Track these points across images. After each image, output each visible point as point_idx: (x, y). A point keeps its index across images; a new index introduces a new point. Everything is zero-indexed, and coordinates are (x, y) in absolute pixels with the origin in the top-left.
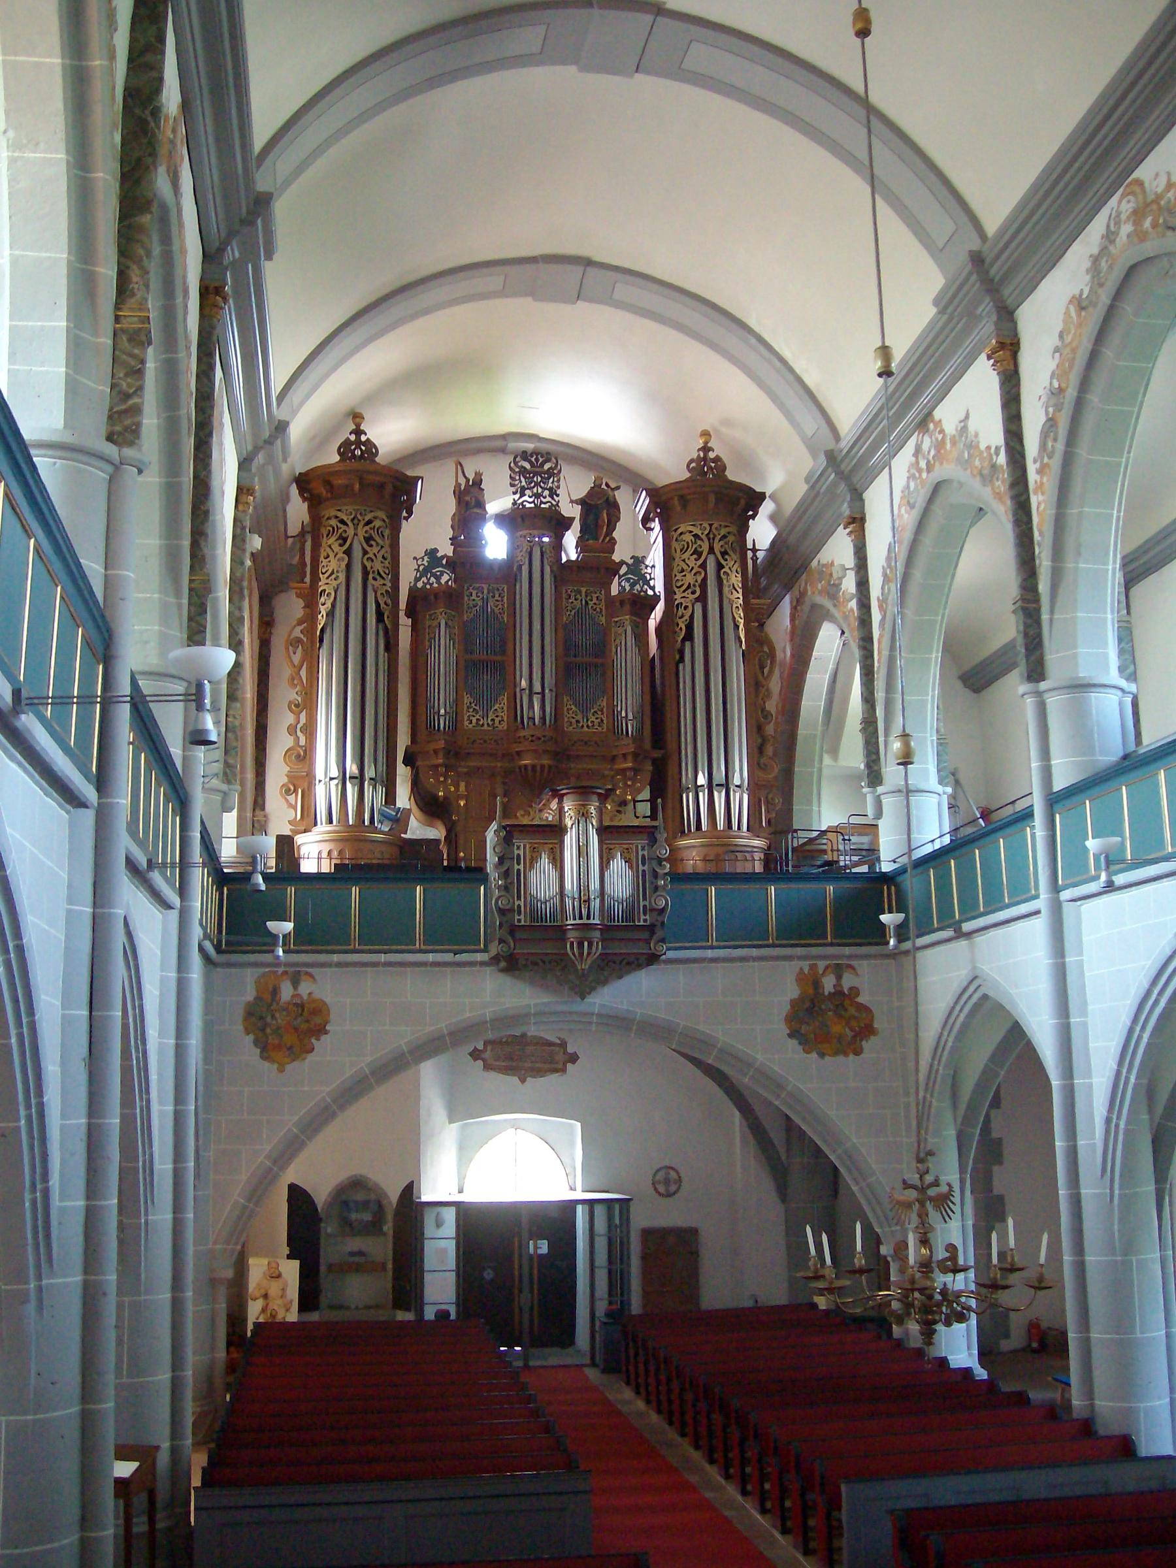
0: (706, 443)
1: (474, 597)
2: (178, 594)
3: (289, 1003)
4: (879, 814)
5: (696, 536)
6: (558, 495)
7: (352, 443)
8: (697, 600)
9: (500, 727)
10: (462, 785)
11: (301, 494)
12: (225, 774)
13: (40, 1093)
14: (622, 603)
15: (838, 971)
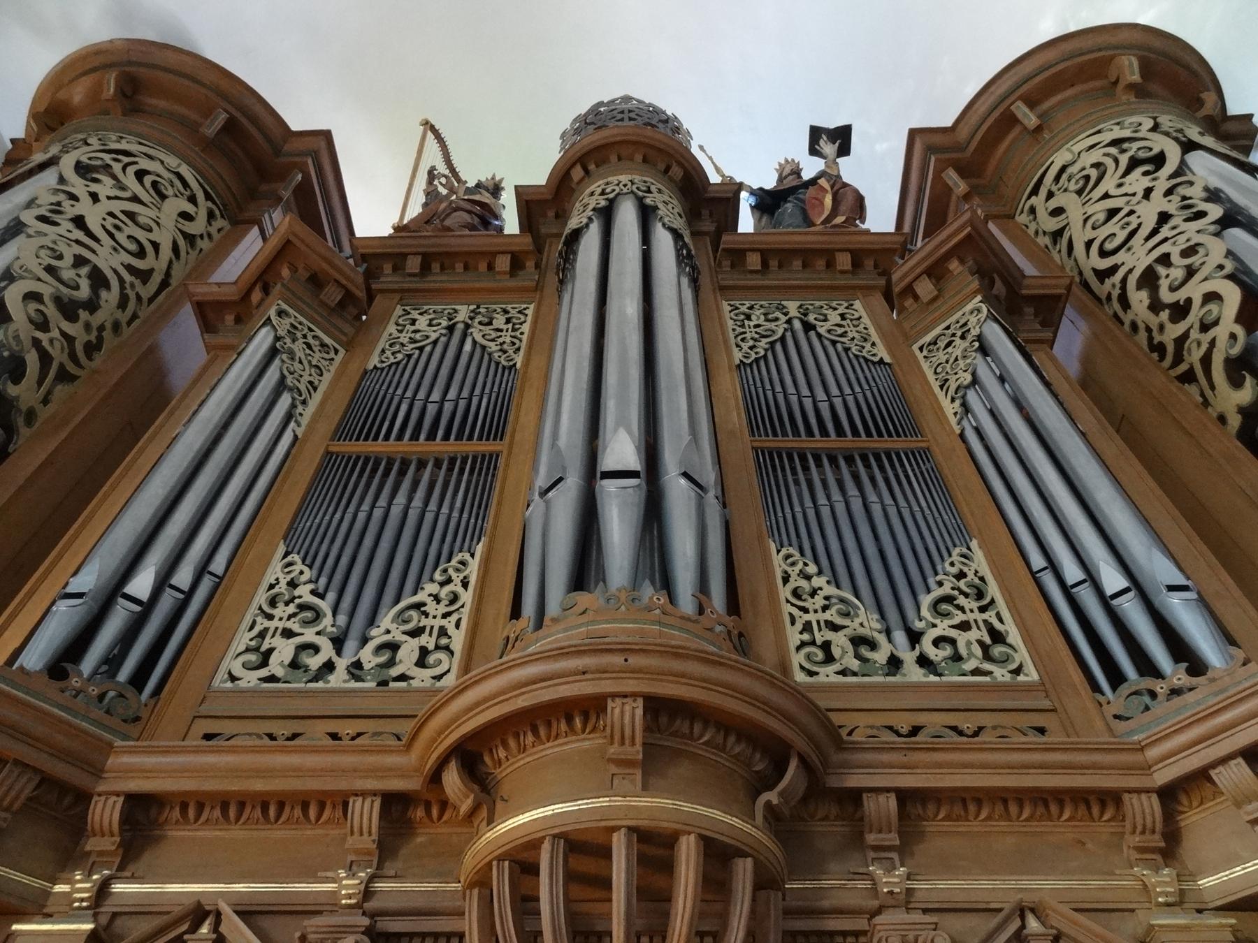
5: (1115, 143)
9: (422, 678)
14: (936, 271)
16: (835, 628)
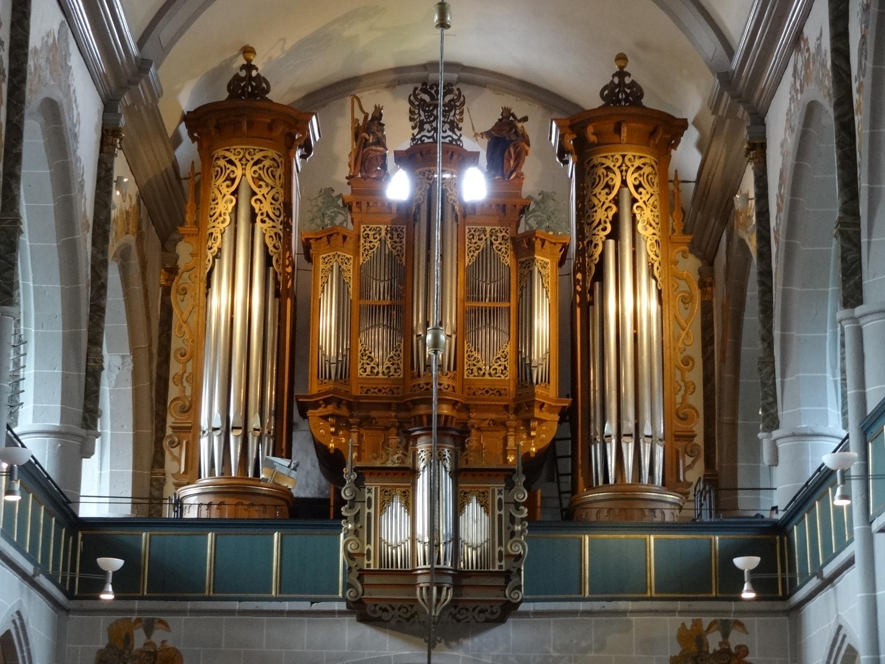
0: (621, 68)
1: (371, 239)
3: (141, 651)
4: (775, 461)
6: (460, 129)
7: (243, 79)
8: (608, 237)
10: (354, 436)
11: (190, 134)
12: (84, 419)
15: (725, 628)
16: (474, 365)
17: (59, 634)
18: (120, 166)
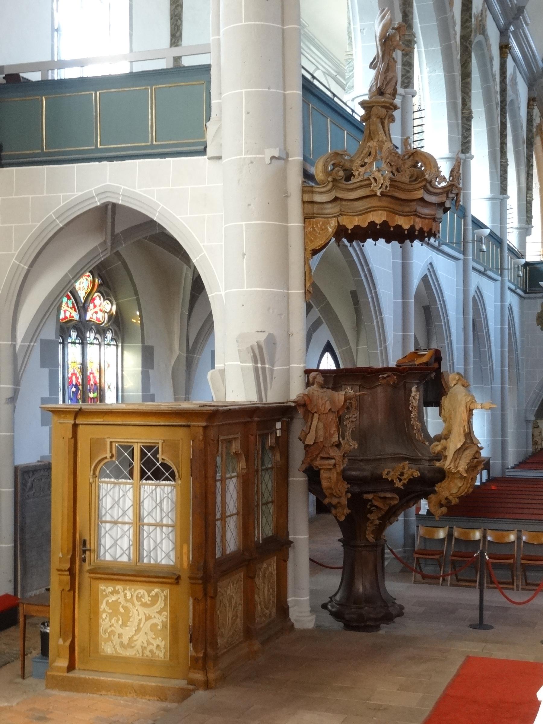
2: (496, 168)
12: (527, 221)
13: (450, 337)
17: (522, 308)
18: (536, 112)
